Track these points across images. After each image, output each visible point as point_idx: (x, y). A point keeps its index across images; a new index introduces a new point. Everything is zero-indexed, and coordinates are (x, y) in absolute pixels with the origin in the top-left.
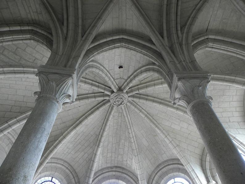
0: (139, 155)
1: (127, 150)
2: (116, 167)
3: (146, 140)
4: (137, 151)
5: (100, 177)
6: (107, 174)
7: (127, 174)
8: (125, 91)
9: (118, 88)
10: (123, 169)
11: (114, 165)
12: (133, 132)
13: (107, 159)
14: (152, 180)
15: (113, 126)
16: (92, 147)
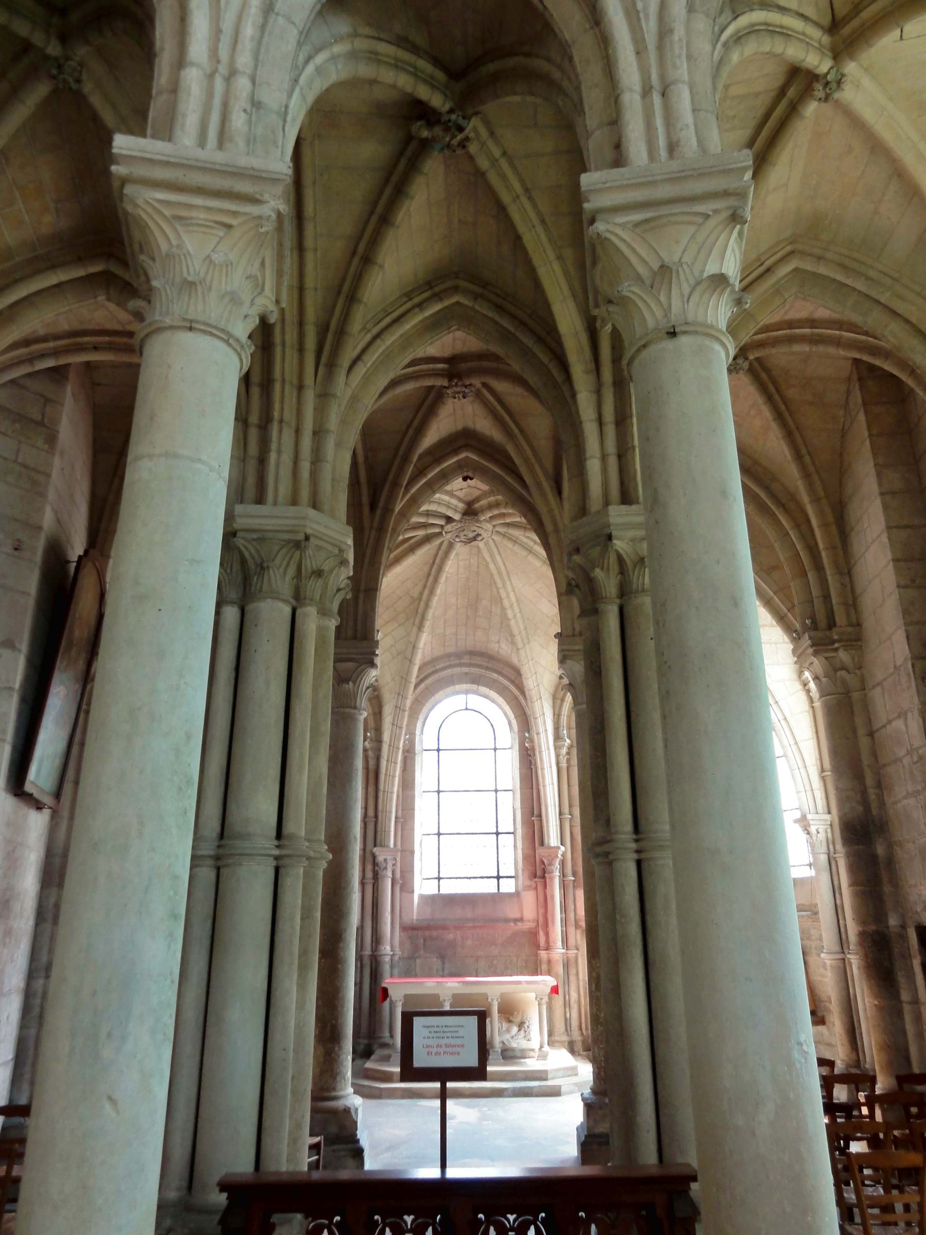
0: (527, 646)
2: (472, 653)
4: (521, 637)
5: (428, 681)
7: (500, 673)
8: (482, 518)
12: (512, 595)
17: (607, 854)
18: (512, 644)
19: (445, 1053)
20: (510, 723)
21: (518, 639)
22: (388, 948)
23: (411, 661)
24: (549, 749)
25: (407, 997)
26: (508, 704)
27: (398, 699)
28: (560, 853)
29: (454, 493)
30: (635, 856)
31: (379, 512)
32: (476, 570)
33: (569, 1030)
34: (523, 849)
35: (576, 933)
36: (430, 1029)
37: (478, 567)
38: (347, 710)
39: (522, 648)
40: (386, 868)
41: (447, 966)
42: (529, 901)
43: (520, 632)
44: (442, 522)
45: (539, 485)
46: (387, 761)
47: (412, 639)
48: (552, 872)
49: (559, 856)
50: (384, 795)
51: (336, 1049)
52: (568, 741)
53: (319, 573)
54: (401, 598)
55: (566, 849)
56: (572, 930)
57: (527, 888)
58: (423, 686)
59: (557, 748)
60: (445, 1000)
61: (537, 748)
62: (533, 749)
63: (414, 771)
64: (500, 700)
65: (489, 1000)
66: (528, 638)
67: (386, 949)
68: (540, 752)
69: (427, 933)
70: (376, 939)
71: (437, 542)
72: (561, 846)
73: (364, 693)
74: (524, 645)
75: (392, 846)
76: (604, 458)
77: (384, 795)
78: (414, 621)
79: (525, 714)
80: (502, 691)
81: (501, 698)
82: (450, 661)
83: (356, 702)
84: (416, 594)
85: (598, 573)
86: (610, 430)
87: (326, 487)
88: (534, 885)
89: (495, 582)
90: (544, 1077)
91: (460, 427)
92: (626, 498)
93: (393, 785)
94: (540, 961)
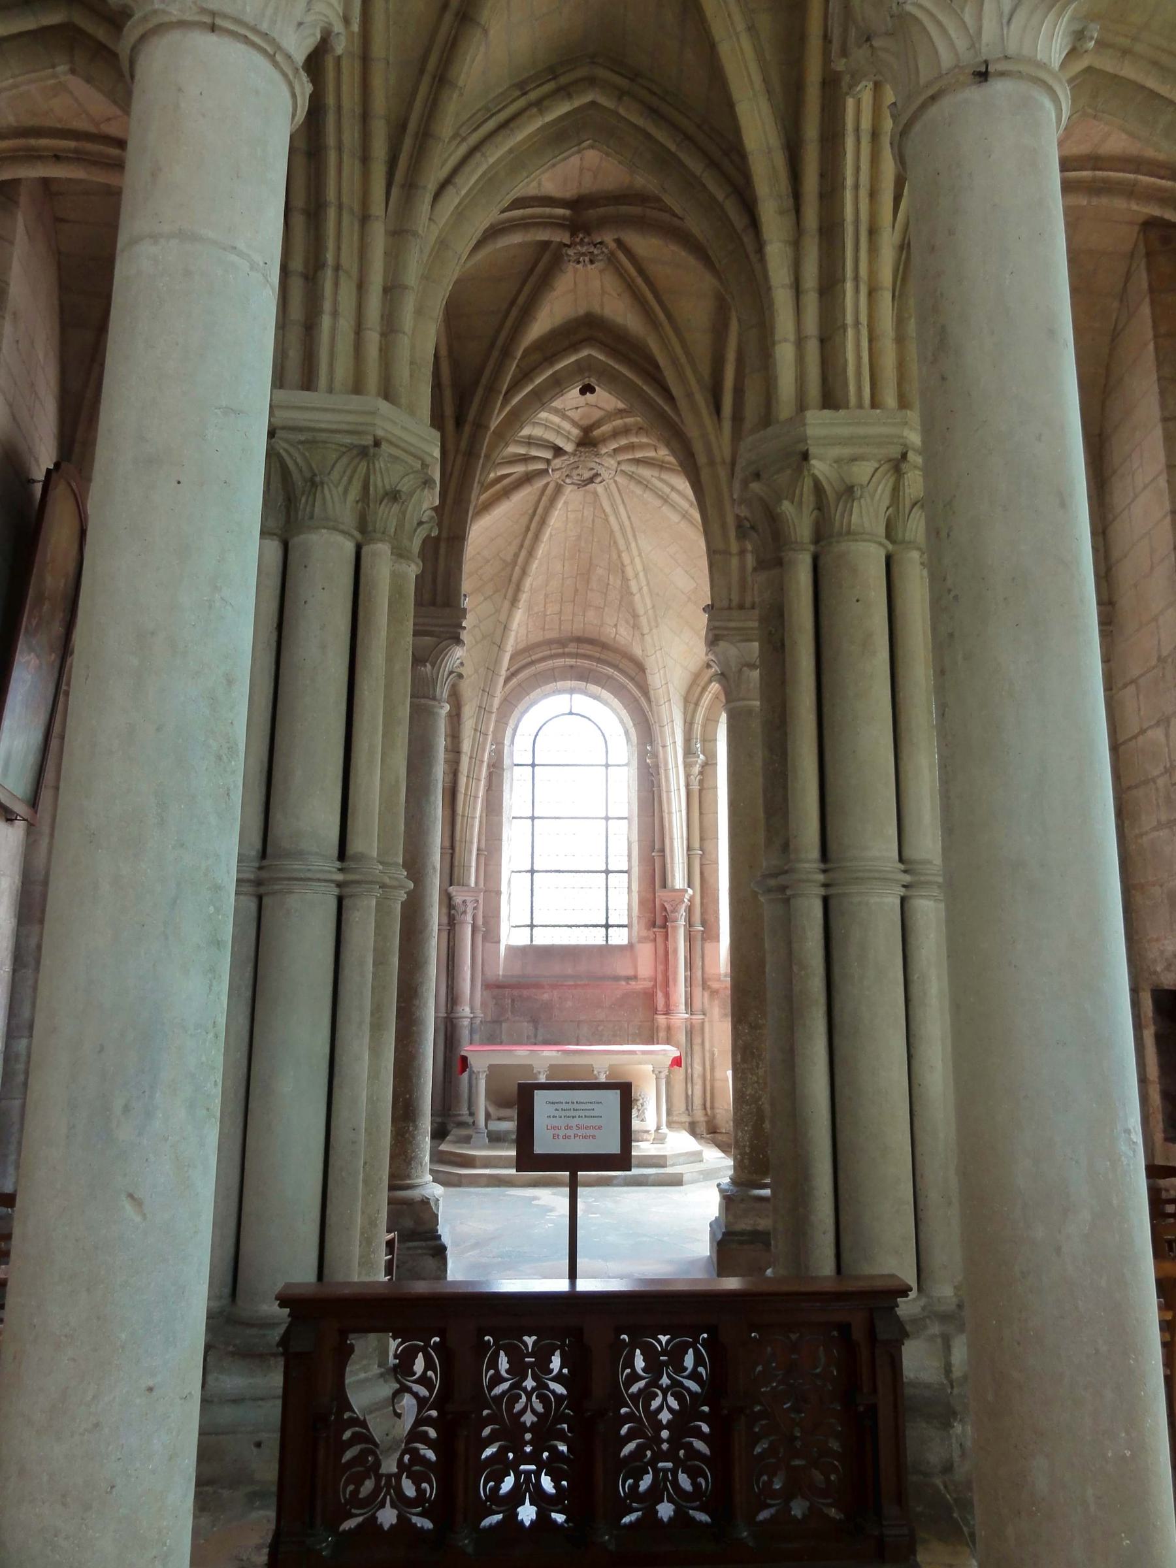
0: (654, 631)
1: (618, 597)
2: (579, 640)
3: (686, 572)
5: (522, 676)
6: (549, 664)
7: (615, 667)
8: (604, 451)
9: (582, 434)
10: (604, 646)
11: (570, 634)
12: (637, 560)
13: (545, 621)
14: (699, 689)
15: (566, 530)
16: (490, 597)
17: (783, 889)
18: (633, 628)
19: (575, 1136)
20: (627, 733)
21: (643, 620)
22: (467, 1009)
23: (500, 647)
24: (677, 767)
25: (491, 1067)
26: (625, 708)
27: (482, 696)
28: (687, 897)
29: (567, 413)
30: (822, 891)
31: (467, 429)
32: (591, 526)
33: (690, 1108)
34: (639, 892)
35: (703, 995)
36: (556, 1106)
37: (593, 521)
38: (423, 701)
39: (647, 634)
40: (465, 912)
41: (541, 1031)
42: (645, 953)
43: (646, 612)
44: (548, 455)
45: (689, 395)
46: (468, 777)
47: (503, 618)
48: (676, 920)
49: (686, 900)
50: (462, 820)
51: (411, 1128)
52: (702, 757)
53: (394, 496)
54: (488, 561)
55: (694, 892)
56: (698, 991)
57: (642, 940)
58: (514, 681)
59: (687, 766)
60: (539, 1072)
61: (662, 765)
62: (657, 766)
63: (502, 792)
64: (616, 702)
65: (595, 1072)
66: (656, 621)
67: (465, 1010)
68: (666, 770)
69: (516, 992)
70: (452, 999)
71: (539, 484)
72: (689, 889)
73: (447, 680)
74: (651, 630)
75: (473, 885)
76: (800, 342)
77: (462, 820)
78: (507, 592)
79: (647, 720)
80: (618, 691)
82: (550, 650)
83: (435, 691)
84: (509, 558)
85: (787, 507)
86: (811, 301)
87: (402, 372)
88: (652, 936)
89: (615, 542)
90: (662, 1163)
91: (581, 312)
92: (831, 399)
93: (474, 808)
94: (657, 1027)
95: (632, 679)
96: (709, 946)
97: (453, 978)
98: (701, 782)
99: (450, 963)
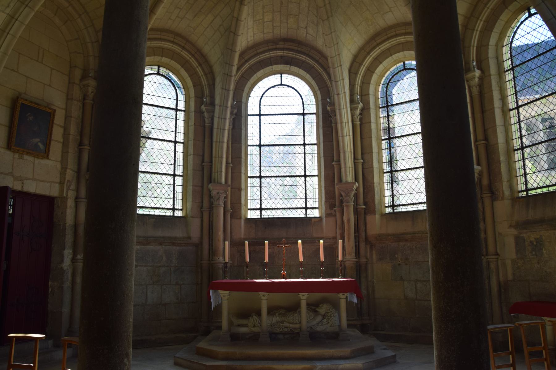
2: (286, 40)
5: (252, 62)
6: (267, 55)
7: (307, 55)
10: (300, 43)
24: (347, 108)
28: (355, 187)
47: (235, 15)
52: (361, 103)
55: (359, 185)
56: (362, 245)
58: (247, 66)
62: (334, 111)
74: (328, 18)
77: (216, 145)
80: (309, 69)
81: (308, 75)
82: (268, 46)
95: (317, 62)
96: (369, 218)
97: (212, 240)
98: (361, 120)
99: (211, 230)
